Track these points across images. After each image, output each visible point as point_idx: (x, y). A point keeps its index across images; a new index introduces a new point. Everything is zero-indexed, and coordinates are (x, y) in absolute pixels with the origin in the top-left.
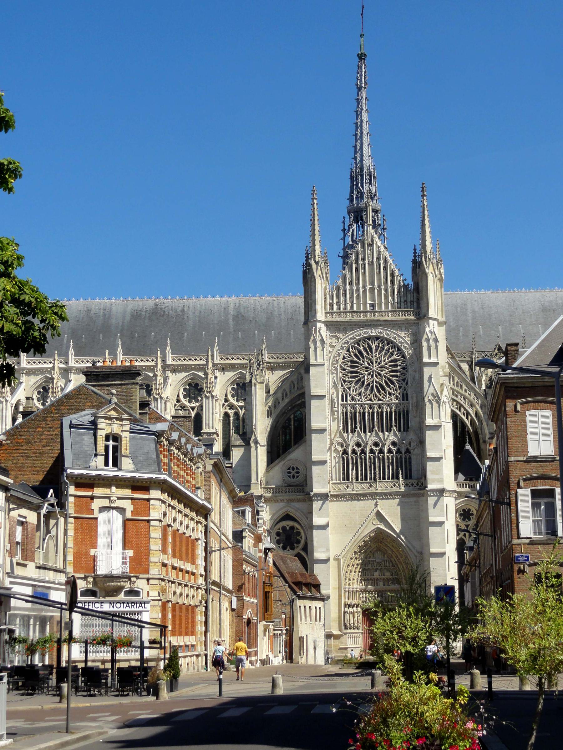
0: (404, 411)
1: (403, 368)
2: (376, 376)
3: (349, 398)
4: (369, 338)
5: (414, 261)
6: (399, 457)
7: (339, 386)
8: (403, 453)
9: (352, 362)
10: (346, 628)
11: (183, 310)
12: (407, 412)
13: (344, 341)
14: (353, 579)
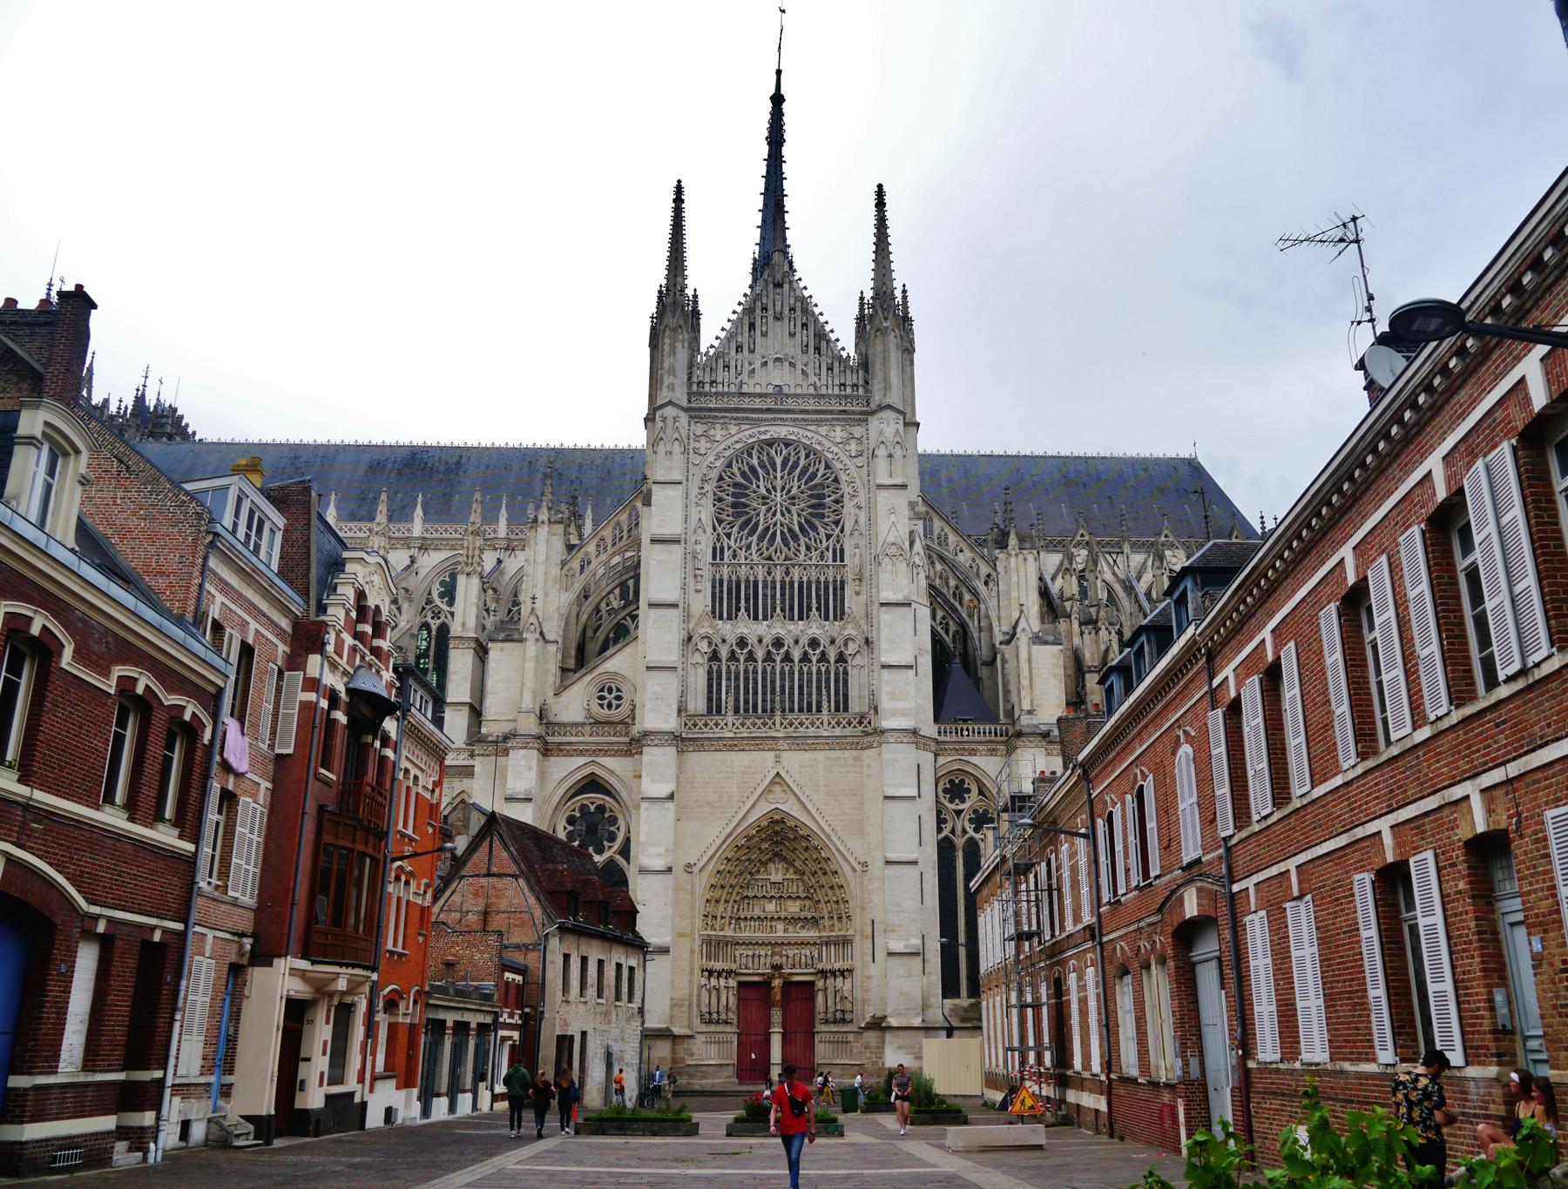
0: (835, 581)
1: (837, 502)
2: (783, 515)
3: (726, 554)
4: (770, 443)
5: (861, 319)
6: (823, 669)
7: (709, 530)
8: (832, 661)
9: (736, 485)
10: (703, 1021)
11: (458, 463)
12: (842, 583)
13: (723, 446)
14: (722, 918)
